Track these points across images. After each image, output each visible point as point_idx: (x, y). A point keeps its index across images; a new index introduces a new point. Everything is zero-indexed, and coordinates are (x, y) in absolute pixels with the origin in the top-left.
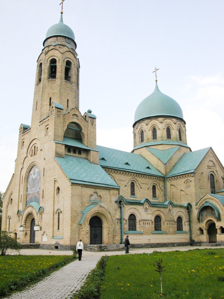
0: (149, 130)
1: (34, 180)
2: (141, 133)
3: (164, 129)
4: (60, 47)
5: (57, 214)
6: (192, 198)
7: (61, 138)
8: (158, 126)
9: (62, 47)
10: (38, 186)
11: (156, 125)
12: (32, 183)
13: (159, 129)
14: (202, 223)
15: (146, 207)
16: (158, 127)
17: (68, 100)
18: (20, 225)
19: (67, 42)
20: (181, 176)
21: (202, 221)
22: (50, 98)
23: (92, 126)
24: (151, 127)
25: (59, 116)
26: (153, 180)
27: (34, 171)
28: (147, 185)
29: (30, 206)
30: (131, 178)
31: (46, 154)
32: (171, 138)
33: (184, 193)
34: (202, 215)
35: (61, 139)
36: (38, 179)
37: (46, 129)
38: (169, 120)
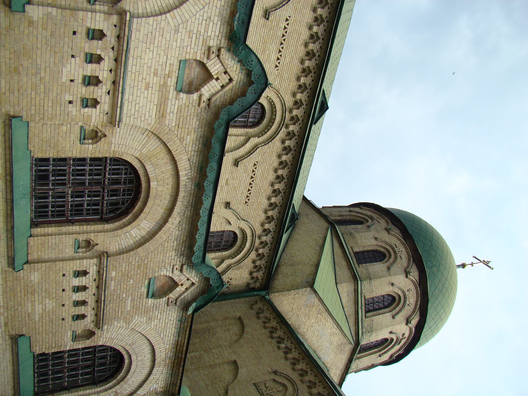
0: (376, 239)
2: (354, 218)
3: (392, 284)
8: (395, 265)
11: (396, 258)
13: (389, 268)
15: (208, 76)
16: (392, 264)
20: (294, 354)
24: (386, 243)
26: (259, 231)
28: (244, 199)
30: (283, 105)
32: (368, 314)
33: (228, 376)
38: (415, 300)
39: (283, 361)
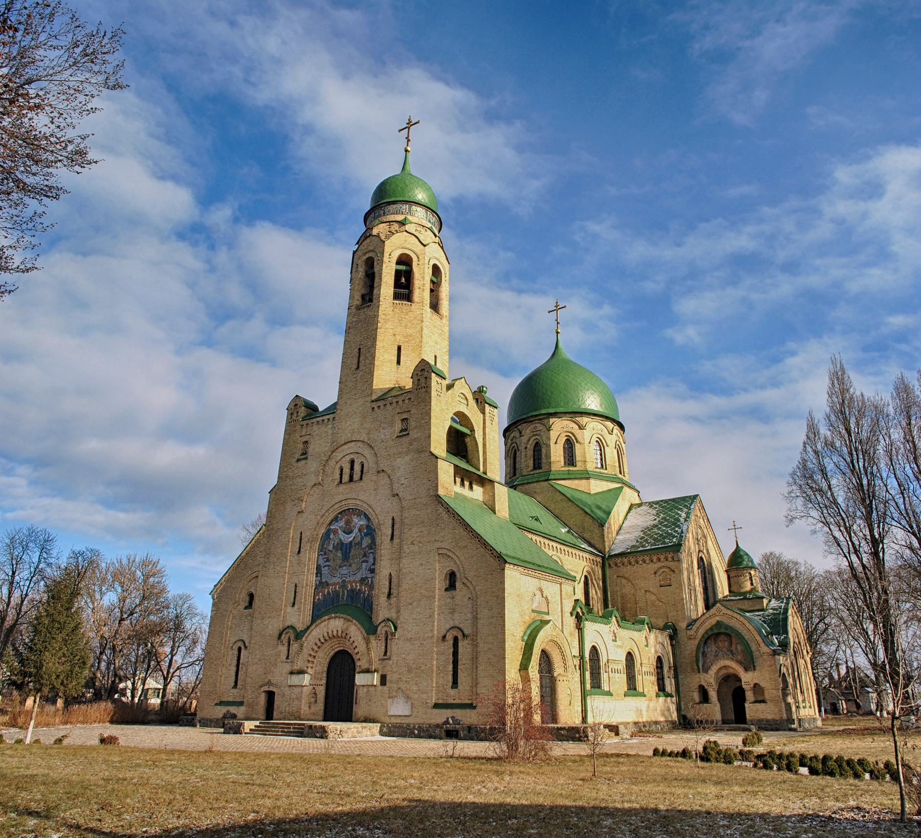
1: (345, 549)
4: (416, 230)
5: (451, 642)
6: (677, 611)
7: (443, 448)
9: (423, 231)
10: (364, 565)
12: (339, 554)
14: (705, 674)
17: (435, 356)
18: (287, 668)
19: (430, 222)
21: (706, 670)
22: (399, 348)
23: (491, 425)
25: (439, 394)
27: (348, 522)
29: (335, 618)
31: (402, 482)
34: (704, 654)
35: (443, 451)
36: (363, 546)
37: (400, 421)
39: (649, 566)
